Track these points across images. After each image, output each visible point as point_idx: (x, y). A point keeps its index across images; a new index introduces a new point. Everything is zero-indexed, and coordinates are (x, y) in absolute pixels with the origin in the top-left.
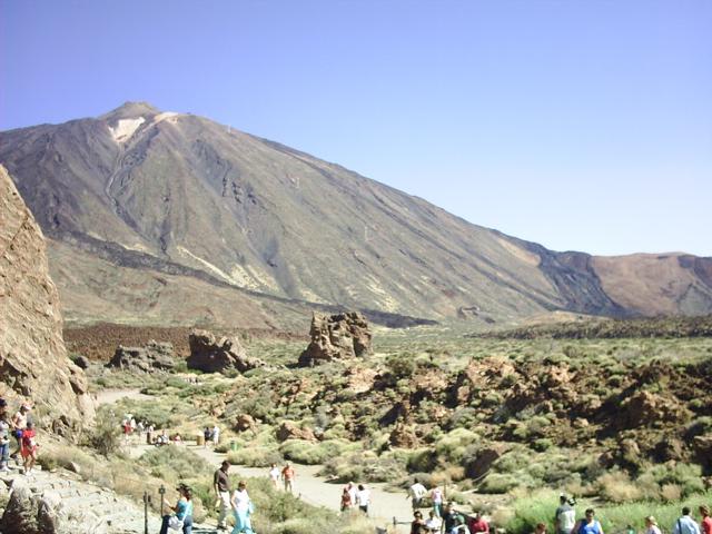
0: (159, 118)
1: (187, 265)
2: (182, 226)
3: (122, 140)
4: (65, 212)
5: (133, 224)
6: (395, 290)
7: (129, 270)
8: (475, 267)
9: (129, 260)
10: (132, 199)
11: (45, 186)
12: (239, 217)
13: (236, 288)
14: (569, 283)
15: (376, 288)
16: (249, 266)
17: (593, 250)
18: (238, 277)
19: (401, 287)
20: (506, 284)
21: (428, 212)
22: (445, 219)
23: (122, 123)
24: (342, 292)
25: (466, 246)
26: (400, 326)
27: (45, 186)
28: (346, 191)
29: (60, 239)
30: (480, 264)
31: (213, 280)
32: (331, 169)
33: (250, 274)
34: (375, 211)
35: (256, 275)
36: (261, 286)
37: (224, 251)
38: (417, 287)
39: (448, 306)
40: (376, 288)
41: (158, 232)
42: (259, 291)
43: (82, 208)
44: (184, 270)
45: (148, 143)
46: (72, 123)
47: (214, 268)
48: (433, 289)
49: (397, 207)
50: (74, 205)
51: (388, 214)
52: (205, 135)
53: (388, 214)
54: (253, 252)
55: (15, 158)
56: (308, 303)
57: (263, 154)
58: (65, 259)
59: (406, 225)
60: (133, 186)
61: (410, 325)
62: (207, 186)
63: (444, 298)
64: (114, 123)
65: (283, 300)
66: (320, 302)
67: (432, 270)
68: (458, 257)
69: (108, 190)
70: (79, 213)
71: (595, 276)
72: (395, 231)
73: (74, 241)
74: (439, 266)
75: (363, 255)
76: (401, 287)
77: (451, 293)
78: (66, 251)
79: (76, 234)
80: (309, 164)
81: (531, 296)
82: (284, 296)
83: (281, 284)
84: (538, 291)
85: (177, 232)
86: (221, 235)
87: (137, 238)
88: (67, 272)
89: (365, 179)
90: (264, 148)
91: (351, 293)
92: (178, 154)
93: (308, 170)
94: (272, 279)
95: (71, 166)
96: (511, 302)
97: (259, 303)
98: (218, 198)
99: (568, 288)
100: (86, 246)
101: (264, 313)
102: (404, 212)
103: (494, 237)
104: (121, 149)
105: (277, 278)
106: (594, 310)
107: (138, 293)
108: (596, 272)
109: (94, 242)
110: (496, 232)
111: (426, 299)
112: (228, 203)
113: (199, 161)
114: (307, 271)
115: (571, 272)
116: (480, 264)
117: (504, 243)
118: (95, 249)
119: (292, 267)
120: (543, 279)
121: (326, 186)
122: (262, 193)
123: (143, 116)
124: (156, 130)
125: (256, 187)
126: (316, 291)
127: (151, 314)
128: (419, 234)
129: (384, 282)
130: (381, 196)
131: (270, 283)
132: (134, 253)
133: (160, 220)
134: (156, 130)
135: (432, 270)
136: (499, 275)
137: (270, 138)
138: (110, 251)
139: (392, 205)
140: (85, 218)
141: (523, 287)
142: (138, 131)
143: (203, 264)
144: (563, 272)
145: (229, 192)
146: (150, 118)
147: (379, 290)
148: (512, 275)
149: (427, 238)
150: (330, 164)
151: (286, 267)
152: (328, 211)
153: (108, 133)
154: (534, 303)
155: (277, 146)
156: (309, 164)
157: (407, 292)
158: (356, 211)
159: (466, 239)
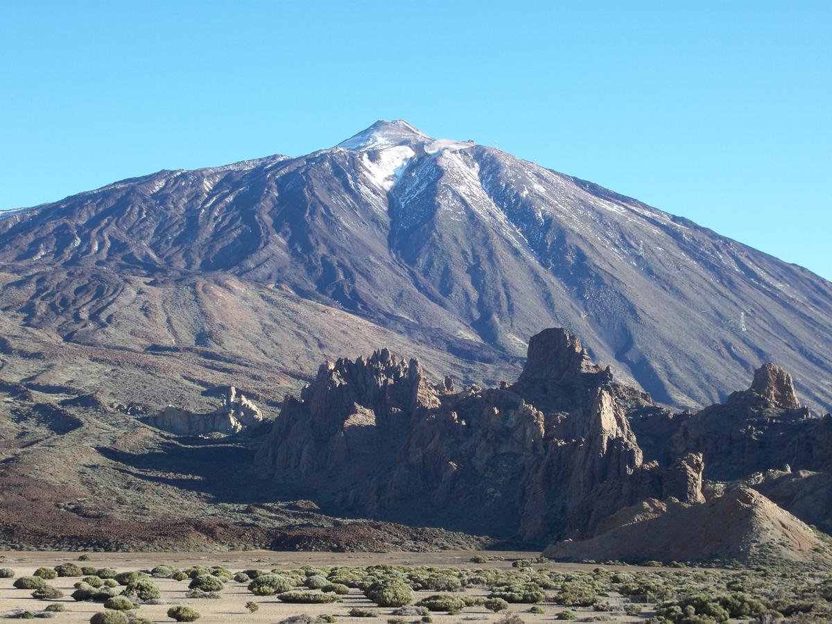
5: (442, 305)
27: (322, 250)
38: (818, 395)
43: (378, 280)
53: (765, 292)
54: (601, 345)
55: (267, 210)
59: (791, 309)
85: (500, 315)
89: (727, 241)
94: (632, 380)
122: (598, 263)
130: (750, 264)
137: (581, 177)
139: (768, 279)
150: (675, 219)
155: (595, 190)
158: (722, 289)
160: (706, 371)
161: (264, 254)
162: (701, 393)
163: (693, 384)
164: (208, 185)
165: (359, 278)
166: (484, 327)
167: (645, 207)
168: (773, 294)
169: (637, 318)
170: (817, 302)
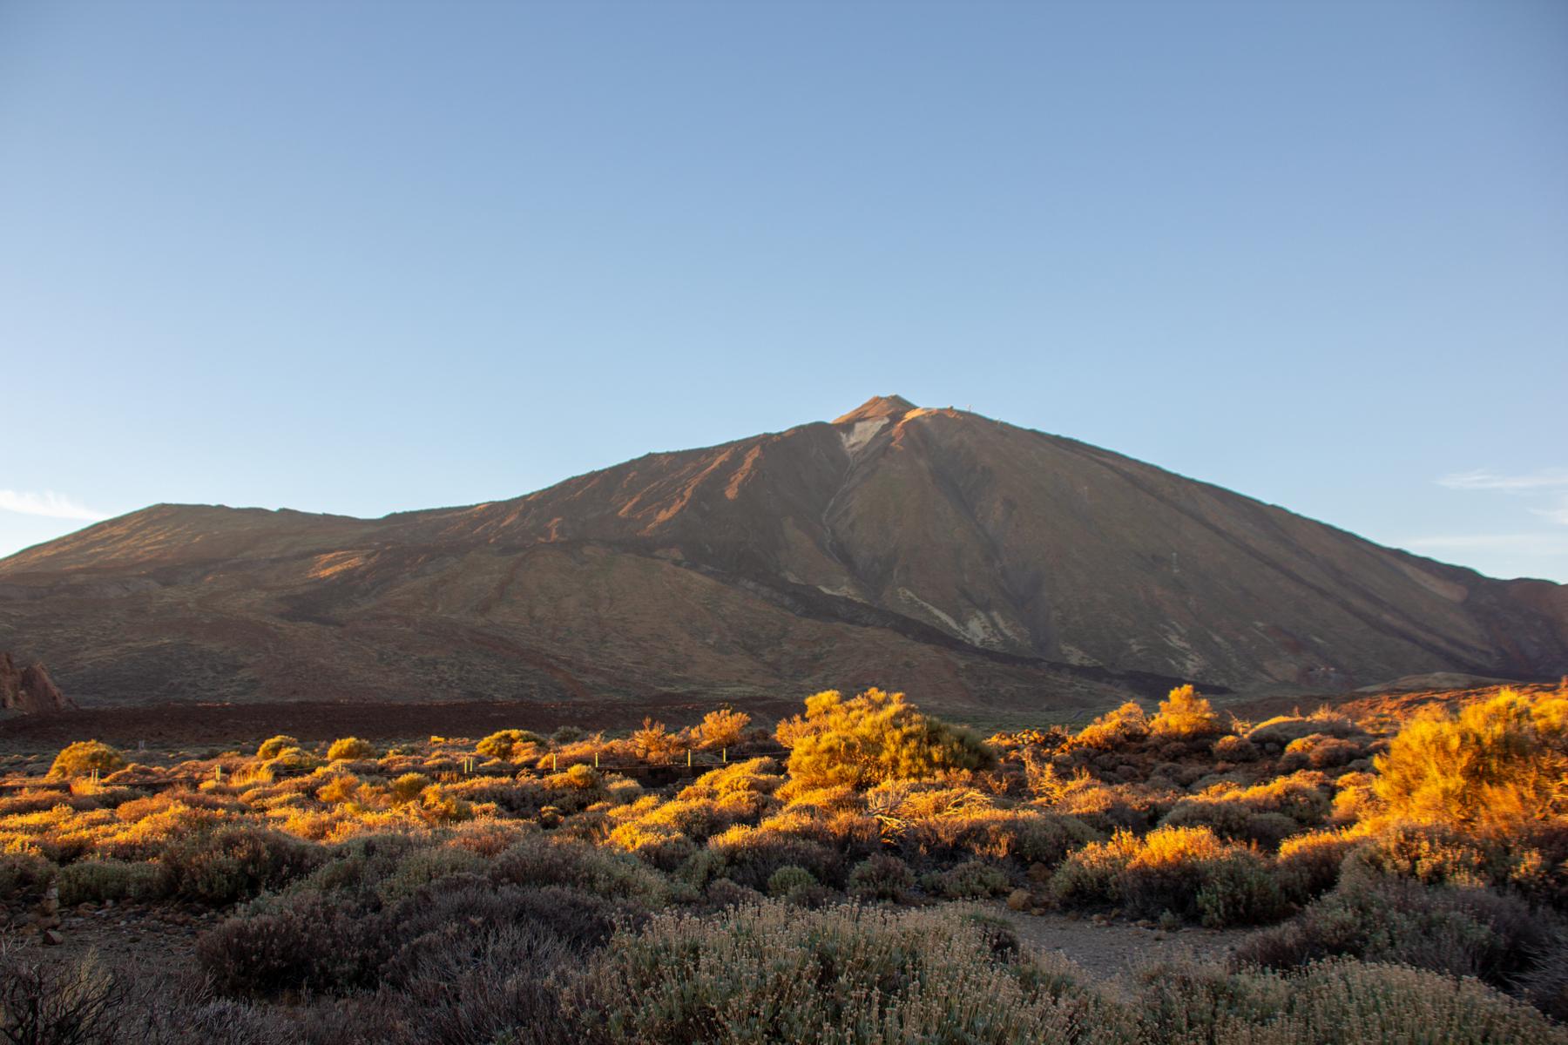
3: (856, 449)
8: (1347, 607)
10: (852, 526)
16: (995, 614)
18: (976, 630)
23: (859, 426)
30: (1357, 602)
33: (994, 625)
35: (1001, 624)
36: (1006, 641)
38: (1242, 638)
40: (1175, 641)
42: (998, 648)
45: (885, 450)
47: (944, 617)
51: (1219, 532)
66: (1086, 663)
68: (1321, 592)
69: (824, 515)
73: (751, 585)
77: (1298, 646)
80: (1111, 467)
87: (846, 579)
91: (1135, 648)
100: (765, 590)
110: (1400, 554)
116: (1357, 602)
117: (1408, 569)
118: (775, 595)
136: (1387, 617)
142: (877, 436)
143: (929, 612)
147: (1183, 644)
153: (838, 441)
156: (1111, 467)
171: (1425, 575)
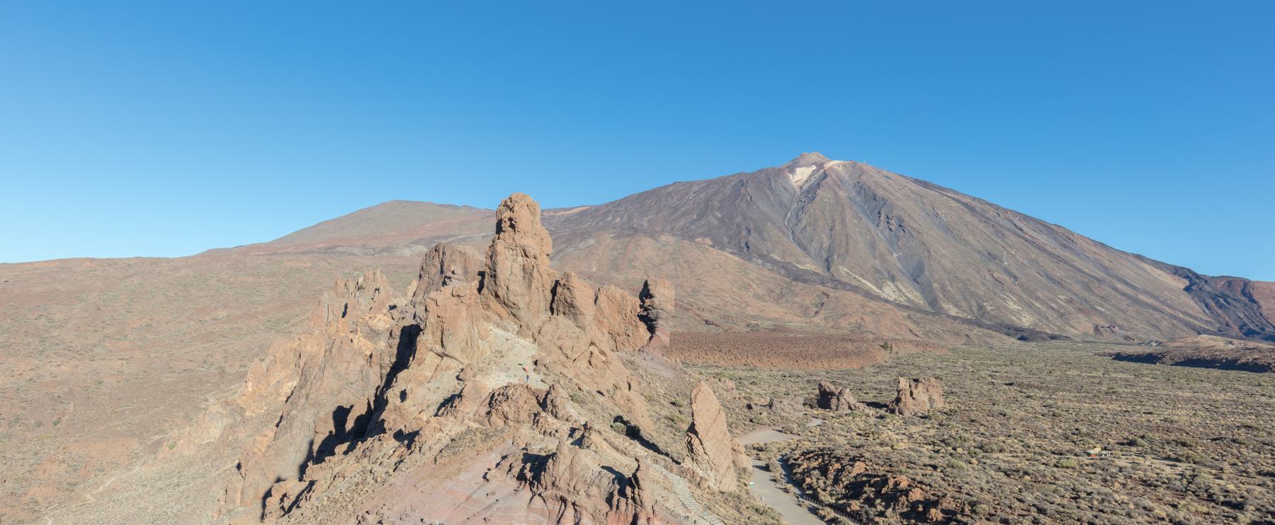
0: (827, 166)
1: (846, 280)
2: (843, 250)
4: (753, 239)
5: (804, 248)
6: (1030, 306)
7: (801, 285)
8: (1116, 289)
9: (800, 277)
10: (804, 228)
11: (739, 219)
12: (890, 243)
13: (887, 301)
14: (1221, 306)
15: (1012, 306)
17: (1252, 278)
18: (889, 291)
19: (1038, 305)
20: (1149, 306)
21: (1066, 239)
22: (1085, 245)
23: (798, 170)
24: (981, 308)
25: (1106, 270)
26: (1032, 340)
27: (739, 219)
28: (988, 221)
29: (750, 260)
30: (1120, 286)
31: (868, 294)
32: (974, 203)
33: (900, 290)
34: (1012, 238)
36: (909, 300)
37: (877, 271)
39: (1081, 325)
40: (1012, 306)
41: (825, 255)
44: (844, 285)
46: (761, 171)
48: (1071, 308)
49: (1034, 234)
50: (760, 233)
51: (1027, 240)
52: (864, 178)
53: (1027, 240)
56: (949, 316)
57: (914, 193)
58: (753, 275)
59: (1045, 251)
60: (805, 219)
61: (1044, 339)
62: (864, 219)
63: (1080, 316)
64: (791, 170)
65: (927, 313)
67: (1069, 290)
68: (1098, 280)
70: (764, 240)
71: (1252, 300)
72: (1033, 256)
73: (760, 261)
74: (1077, 288)
75: (1004, 277)
76: (1038, 305)
78: (755, 270)
79: (761, 256)
81: (1176, 318)
82: (929, 309)
83: (925, 298)
84: (1185, 313)
86: (875, 258)
88: (754, 286)
89: (1006, 211)
90: (915, 187)
91: (989, 308)
92: (842, 194)
93: (953, 204)
94: (918, 294)
95: (760, 204)
96: (1154, 322)
97: (905, 314)
98: (872, 227)
99: (1220, 311)
101: (909, 323)
102: (1042, 239)
103: (1138, 262)
104: (798, 191)
105: (922, 293)
106: (1250, 334)
107: (807, 302)
108: (1255, 297)
109: (774, 262)
110: (1139, 257)
111: (1062, 316)
112: (882, 232)
113: (858, 199)
114: (949, 288)
115: (1225, 297)
116: (1120, 286)
119: (935, 285)
120: (1192, 303)
121: (968, 217)
123: (815, 164)
124: (825, 176)
125: (906, 219)
126: (956, 306)
127: (817, 320)
128: (1058, 259)
129: (1021, 300)
131: (916, 297)
132: (805, 271)
133: (826, 245)
134: (825, 176)
135: (1069, 290)
136: (1142, 297)
138: (787, 270)
139: (1031, 233)
140: (769, 245)
141: (1168, 310)
144: (1215, 298)
145: (883, 225)
146: (820, 166)
148: (1155, 297)
149: (1066, 262)
151: (930, 284)
152: (971, 238)
153: (787, 178)
154: (1180, 325)
155: (925, 184)
157: (1043, 308)
159: (1107, 264)
160: (972, 289)
161: (703, 222)
162: (963, 304)
163: (959, 297)
164: (695, 188)
165: (753, 234)
166: (828, 264)
167: (956, 192)
168: (1032, 242)
169: (930, 256)
170: (1065, 247)
171: (1159, 272)
